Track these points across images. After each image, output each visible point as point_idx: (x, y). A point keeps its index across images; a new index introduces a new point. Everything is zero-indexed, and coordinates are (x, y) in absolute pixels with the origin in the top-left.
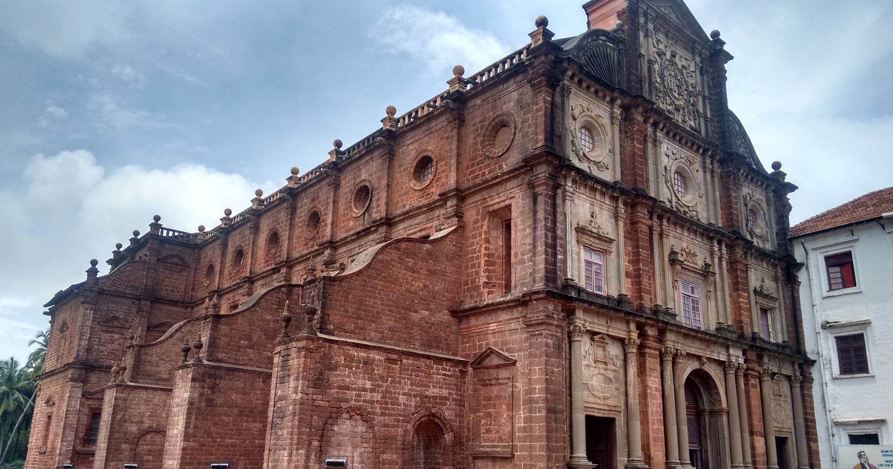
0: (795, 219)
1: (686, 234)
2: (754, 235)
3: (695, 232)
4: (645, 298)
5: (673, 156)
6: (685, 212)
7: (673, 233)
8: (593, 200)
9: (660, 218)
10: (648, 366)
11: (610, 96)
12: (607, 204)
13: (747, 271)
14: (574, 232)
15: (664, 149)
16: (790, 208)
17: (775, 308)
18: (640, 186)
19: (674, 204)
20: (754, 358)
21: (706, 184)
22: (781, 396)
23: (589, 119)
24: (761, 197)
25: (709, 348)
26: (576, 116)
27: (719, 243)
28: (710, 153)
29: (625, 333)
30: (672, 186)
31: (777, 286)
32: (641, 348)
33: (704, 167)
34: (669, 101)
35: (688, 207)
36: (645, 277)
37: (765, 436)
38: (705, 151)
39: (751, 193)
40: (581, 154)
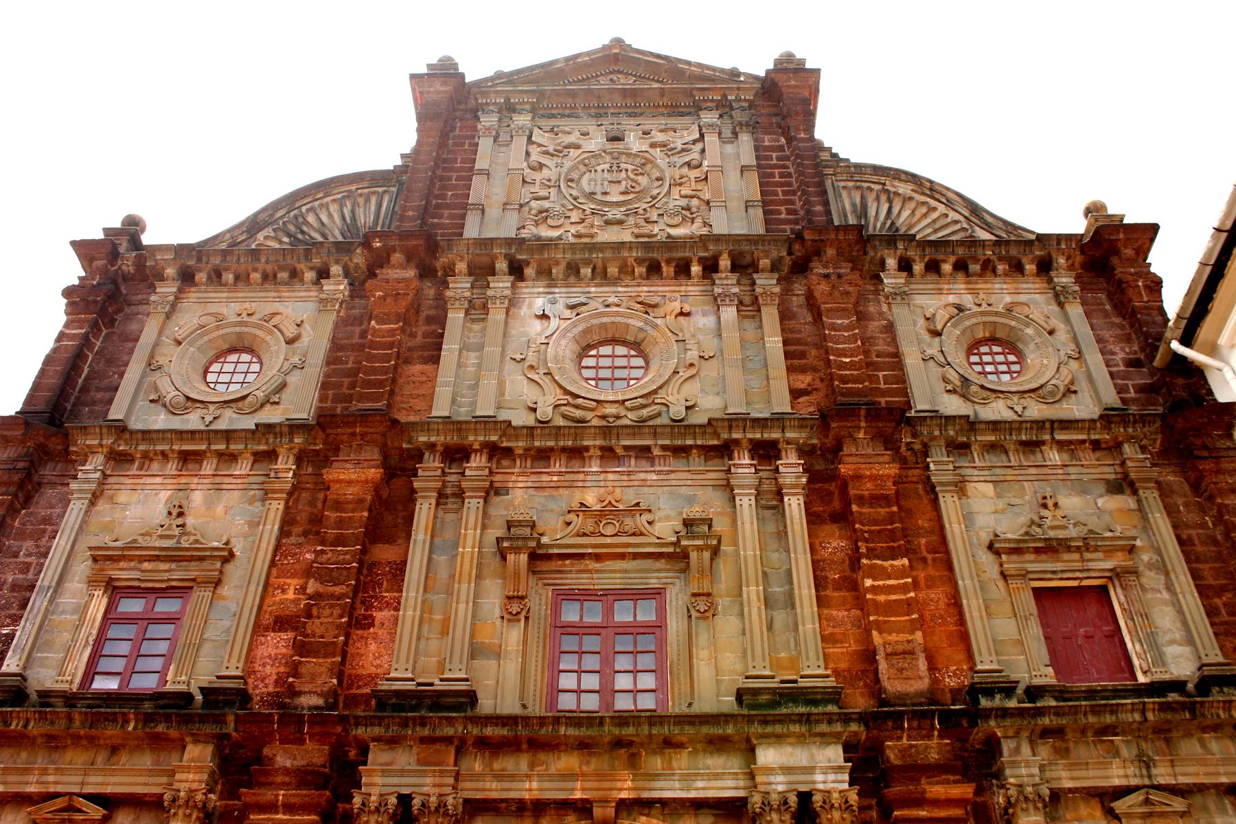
1: (594, 469)
2: (985, 394)
4: (303, 670)
5: (568, 313)
6: (604, 417)
7: (534, 478)
8: (183, 480)
11: (312, 269)
12: (240, 476)
13: (936, 495)
14: (82, 567)
15: (530, 306)
16: (1156, 284)
17: (1135, 572)
21: (719, 333)
23: (238, 329)
24: (1023, 298)
25: (633, 762)
26: (179, 338)
27: (766, 452)
28: (725, 262)
29: (164, 780)
31: (1139, 501)
33: (717, 302)
34: (575, 216)
35: (624, 401)
36: (327, 612)
38: (710, 267)
39: (968, 300)
40: (170, 394)
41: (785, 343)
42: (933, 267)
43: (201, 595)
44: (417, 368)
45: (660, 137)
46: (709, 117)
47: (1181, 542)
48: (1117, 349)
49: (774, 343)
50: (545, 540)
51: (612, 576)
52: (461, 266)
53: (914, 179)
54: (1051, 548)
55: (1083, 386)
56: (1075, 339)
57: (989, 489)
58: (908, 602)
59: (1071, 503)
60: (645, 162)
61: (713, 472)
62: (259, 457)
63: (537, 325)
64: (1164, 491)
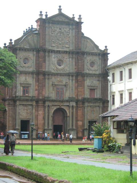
0: (110, 62)
3: (63, 75)
5: (56, 58)
9: (49, 75)
10: (39, 109)
16: (108, 59)
18: (40, 69)
19: (55, 70)
20: (81, 103)
21: (69, 61)
22: (94, 111)
27: (72, 76)
28: (71, 53)
30: (55, 65)
32: (37, 106)
33: (69, 58)
37: (83, 121)
38: (69, 53)
40: (22, 66)
41: (75, 62)
42: (89, 54)
43: (30, 88)
44: (44, 64)
45: (65, 29)
46: (70, 27)
47: (101, 86)
48: (103, 65)
49: (74, 63)
50: (55, 83)
51: (60, 87)
52: (47, 51)
53: (91, 40)
54: (92, 86)
55: (98, 70)
56: (99, 64)
57: (88, 80)
58: (81, 91)
59: (94, 82)
60: (63, 34)
61: (67, 77)
62: (32, 74)
63: (53, 59)
64: (102, 81)
